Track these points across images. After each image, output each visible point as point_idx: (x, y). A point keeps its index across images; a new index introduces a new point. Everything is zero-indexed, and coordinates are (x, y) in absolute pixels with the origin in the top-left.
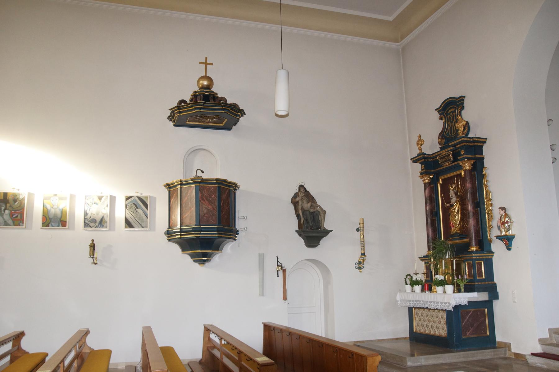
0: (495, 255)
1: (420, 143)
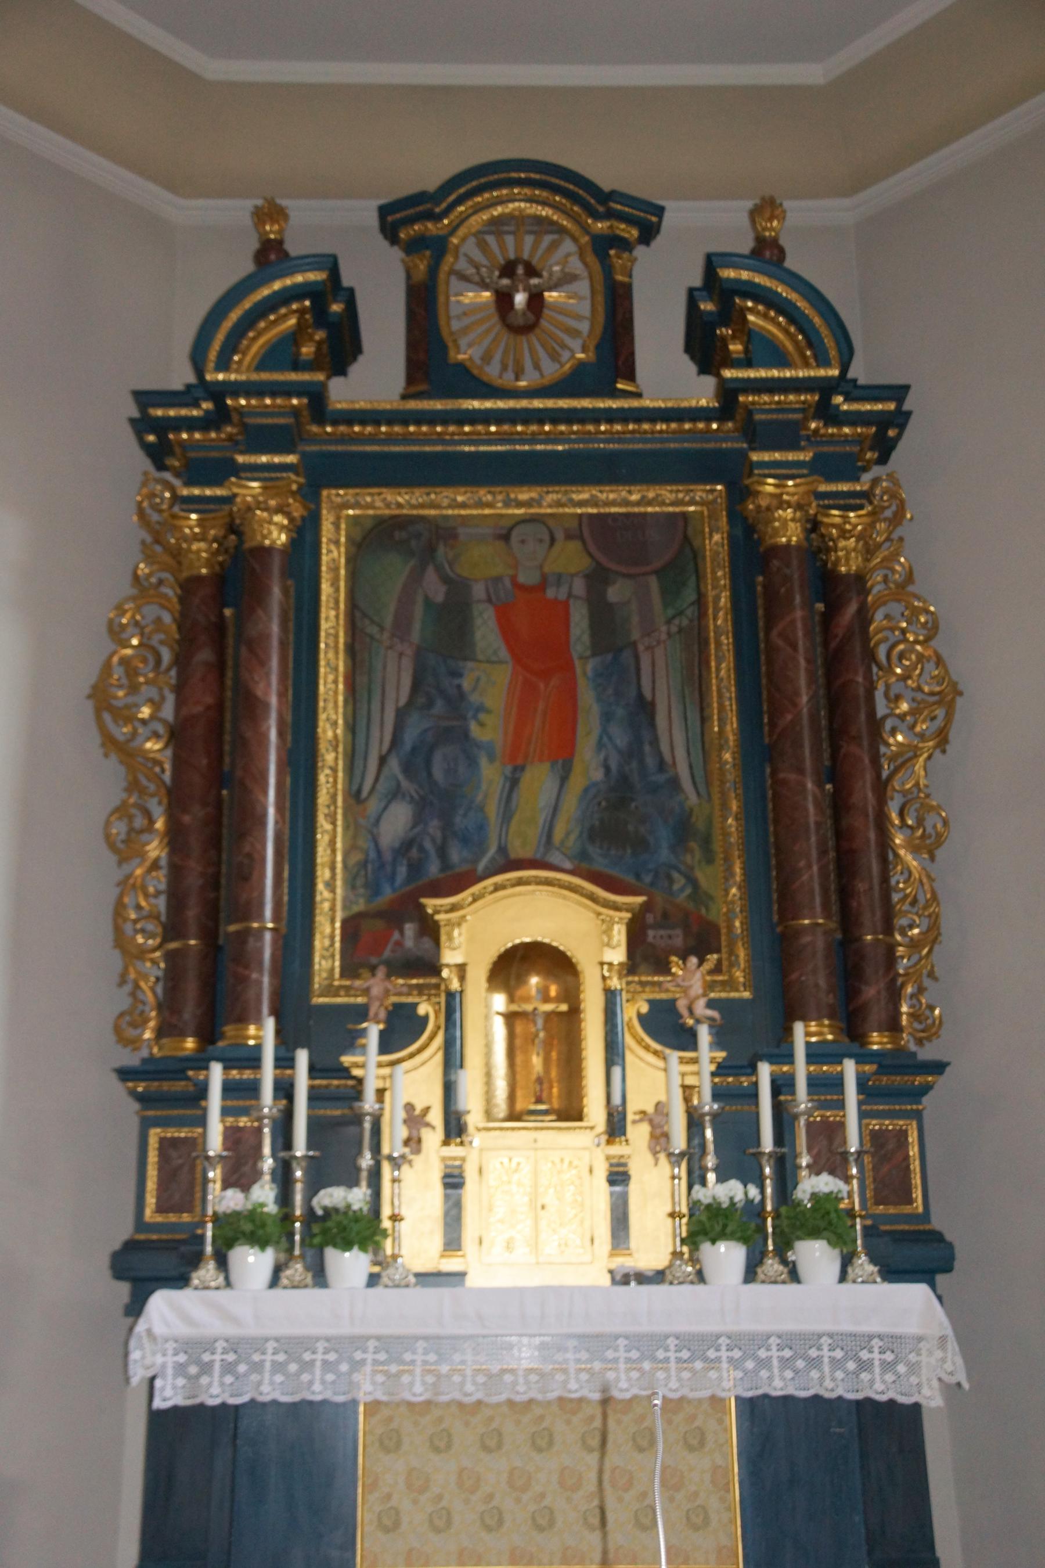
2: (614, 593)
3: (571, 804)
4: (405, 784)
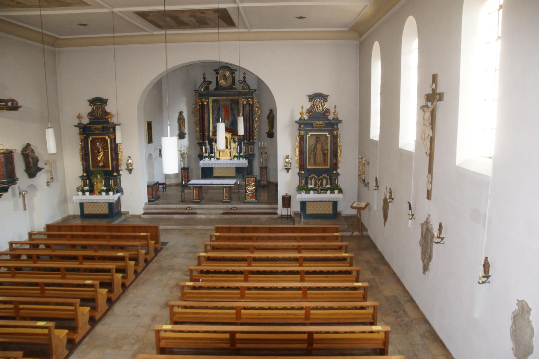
0: (122, 176)
1: (79, 117)
3: (229, 123)
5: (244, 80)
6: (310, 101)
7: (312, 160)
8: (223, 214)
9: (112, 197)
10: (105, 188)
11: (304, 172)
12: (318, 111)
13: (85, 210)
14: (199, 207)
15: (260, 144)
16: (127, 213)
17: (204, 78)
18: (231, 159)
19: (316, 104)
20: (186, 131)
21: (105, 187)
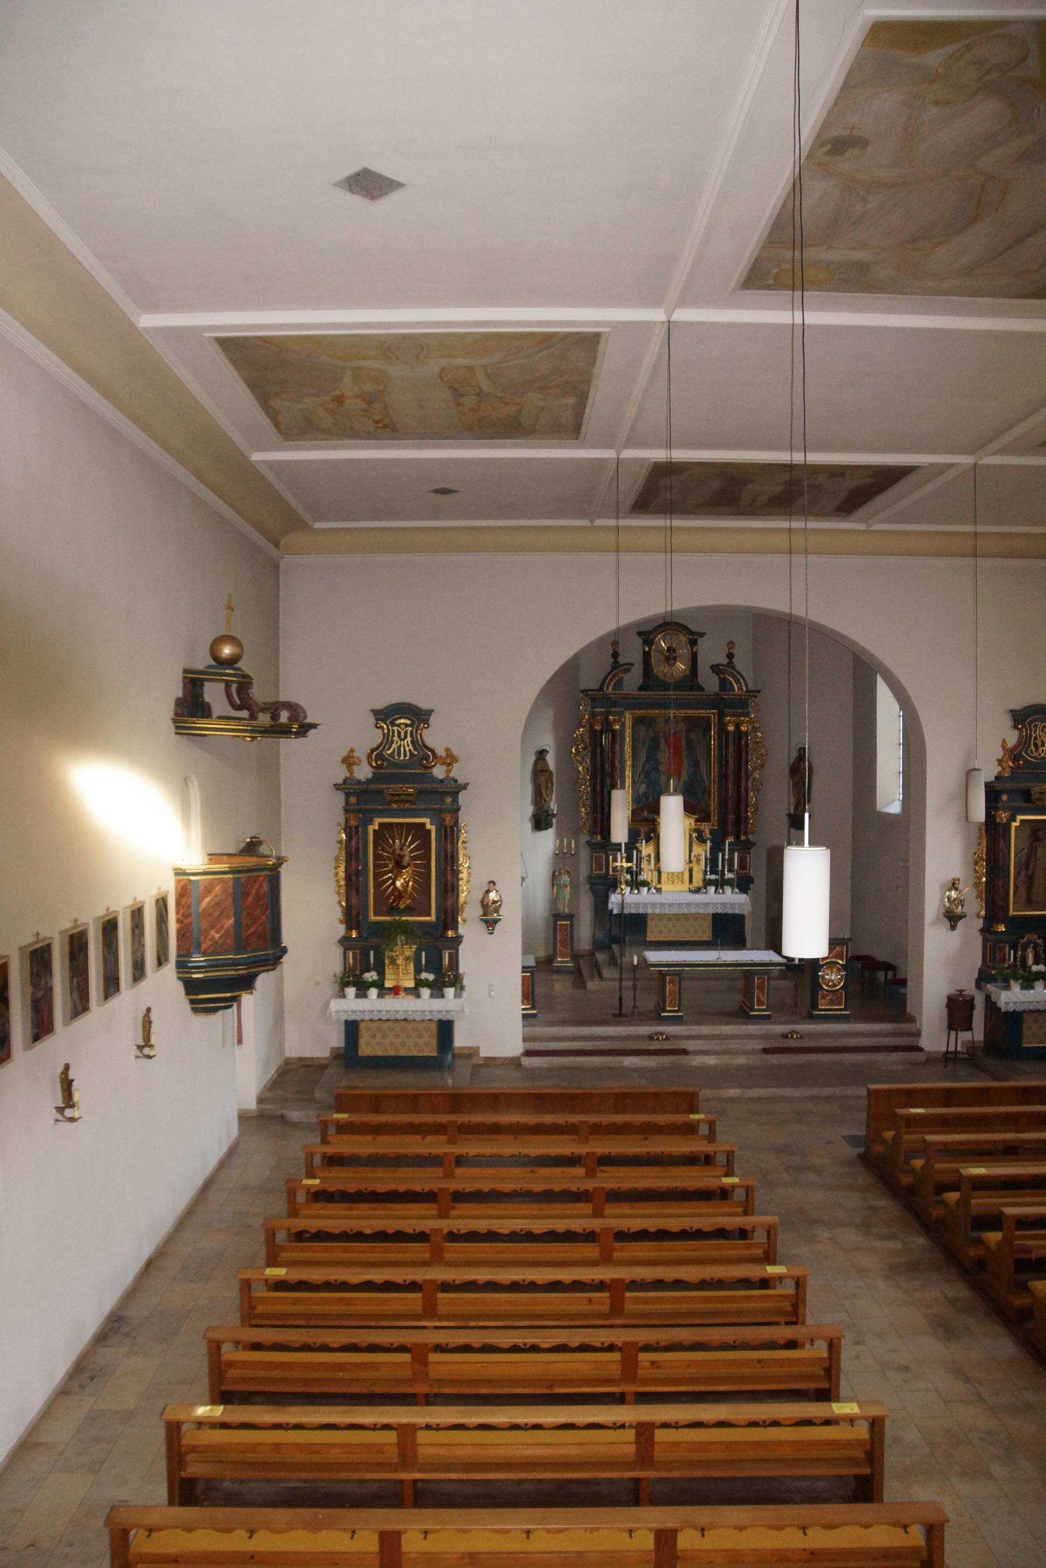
1: (349, 761)
2: (692, 735)
4: (645, 780)
5: (728, 663)
6: (1015, 727)
7: (1022, 891)
8: (766, 1051)
9: (448, 1003)
10: (431, 977)
11: (1005, 927)
12: (1040, 755)
13: (362, 1042)
14: (686, 1033)
15: (573, 846)
16: (471, 1053)
17: (615, 655)
18: (698, 891)
19: (1034, 736)
20: (553, 806)
21: (428, 971)
